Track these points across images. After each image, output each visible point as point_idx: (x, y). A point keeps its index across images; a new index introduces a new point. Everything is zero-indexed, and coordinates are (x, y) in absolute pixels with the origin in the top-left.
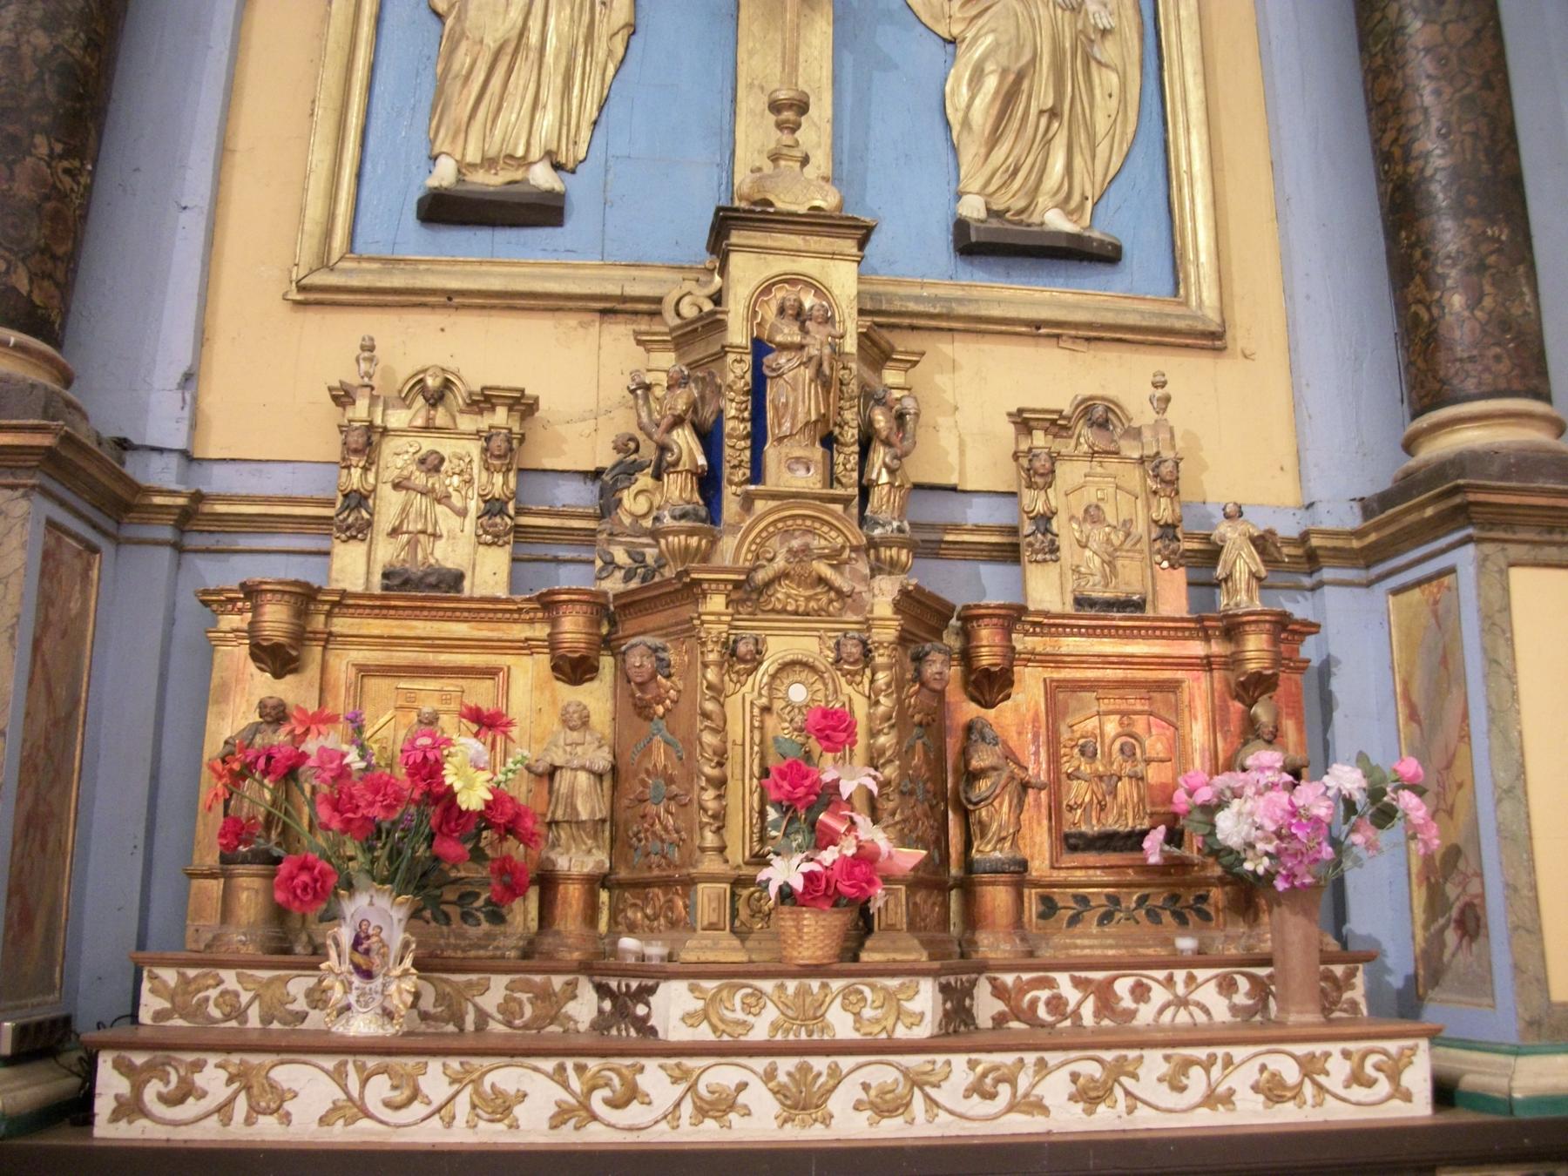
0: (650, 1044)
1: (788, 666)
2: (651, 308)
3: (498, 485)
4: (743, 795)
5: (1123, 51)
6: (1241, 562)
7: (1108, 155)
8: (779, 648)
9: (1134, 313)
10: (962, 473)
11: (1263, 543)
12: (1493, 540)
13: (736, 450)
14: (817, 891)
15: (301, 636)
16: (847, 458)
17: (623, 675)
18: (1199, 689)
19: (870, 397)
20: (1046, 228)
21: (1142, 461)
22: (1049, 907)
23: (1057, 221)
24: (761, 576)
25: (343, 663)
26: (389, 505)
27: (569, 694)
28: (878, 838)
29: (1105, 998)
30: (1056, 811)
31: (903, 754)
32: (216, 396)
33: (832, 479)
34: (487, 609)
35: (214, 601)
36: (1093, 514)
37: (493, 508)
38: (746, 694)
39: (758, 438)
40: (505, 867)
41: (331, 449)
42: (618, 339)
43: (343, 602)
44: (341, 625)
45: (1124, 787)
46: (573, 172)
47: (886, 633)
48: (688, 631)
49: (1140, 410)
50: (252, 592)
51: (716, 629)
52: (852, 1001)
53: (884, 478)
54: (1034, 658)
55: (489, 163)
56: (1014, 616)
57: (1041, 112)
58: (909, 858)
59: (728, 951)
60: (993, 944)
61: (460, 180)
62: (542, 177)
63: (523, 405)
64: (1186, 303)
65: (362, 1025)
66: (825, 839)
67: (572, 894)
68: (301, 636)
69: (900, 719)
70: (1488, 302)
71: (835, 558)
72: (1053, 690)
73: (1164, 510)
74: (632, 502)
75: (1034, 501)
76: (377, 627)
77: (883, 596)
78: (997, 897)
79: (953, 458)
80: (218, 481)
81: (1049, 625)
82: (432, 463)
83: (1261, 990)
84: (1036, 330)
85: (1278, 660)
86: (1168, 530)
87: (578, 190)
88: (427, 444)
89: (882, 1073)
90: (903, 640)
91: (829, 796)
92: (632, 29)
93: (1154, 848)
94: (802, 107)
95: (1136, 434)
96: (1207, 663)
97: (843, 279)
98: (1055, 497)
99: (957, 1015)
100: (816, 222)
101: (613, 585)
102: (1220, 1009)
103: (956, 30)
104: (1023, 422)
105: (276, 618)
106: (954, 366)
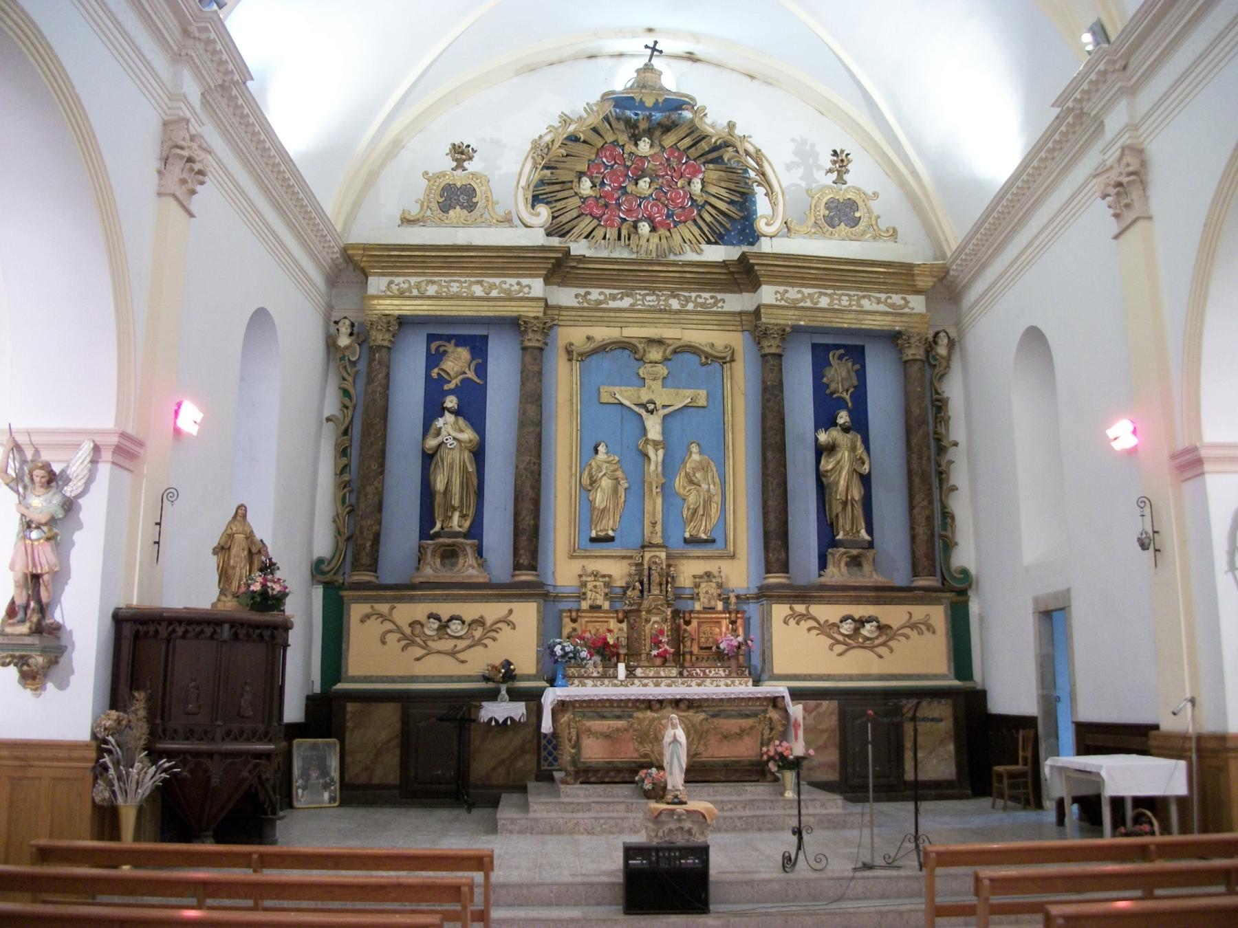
0: (635, 677)
1: (655, 622)
2: (631, 557)
3: (607, 590)
4: (648, 641)
5: (717, 499)
6: (733, 600)
7: (714, 520)
8: (654, 619)
9: (717, 553)
11: (738, 597)
13: (646, 586)
14: (659, 655)
15: (578, 616)
16: (664, 586)
17: (628, 622)
18: (725, 623)
19: (668, 575)
22: (697, 659)
23: (704, 536)
25: (584, 620)
26: (589, 594)
27: (620, 625)
28: (668, 648)
29: (704, 672)
30: (699, 643)
31: (672, 635)
32: (557, 575)
33: (661, 591)
34: (606, 612)
35: (562, 611)
36: (707, 592)
37: (606, 594)
38: (648, 627)
39: (649, 584)
40: (612, 652)
41: (578, 584)
42: (625, 563)
43: (584, 611)
44: (583, 614)
45: (711, 640)
47: (669, 617)
48: (639, 617)
49: (716, 574)
50: (570, 611)
51: (644, 617)
52: (664, 671)
54: (695, 618)
56: (691, 612)
58: (672, 650)
59: (647, 664)
60: (687, 664)
62: (611, 533)
63: (610, 576)
65: (595, 674)
66: (659, 648)
67: (622, 657)
68: (578, 616)
69: (672, 630)
71: (662, 605)
72: (699, 623)
73: (719, 591)
74: (629, 593)
75: (696, 591)
76: (589, 615)
77: (669, 611)
78: (688, 657)
80: (559, 590)
81: (699, 612)
82: (595, 587)
83: (730, 672)
85: (737, 618)
86: (720, 595)
88: (595, 583)
89: (668, 681)
90: (673, 617)
91: (661, 642)
93: (714, 649)
94: (656, 523)
95: (715, 577)
96: (725, 618)
97: (663, 555)
98: (700, 590)
99: (681, 674)
100: (657, 546)
101: (626, 608)
102: (723, 675)
104: (694, 577)
105: (574, 614)
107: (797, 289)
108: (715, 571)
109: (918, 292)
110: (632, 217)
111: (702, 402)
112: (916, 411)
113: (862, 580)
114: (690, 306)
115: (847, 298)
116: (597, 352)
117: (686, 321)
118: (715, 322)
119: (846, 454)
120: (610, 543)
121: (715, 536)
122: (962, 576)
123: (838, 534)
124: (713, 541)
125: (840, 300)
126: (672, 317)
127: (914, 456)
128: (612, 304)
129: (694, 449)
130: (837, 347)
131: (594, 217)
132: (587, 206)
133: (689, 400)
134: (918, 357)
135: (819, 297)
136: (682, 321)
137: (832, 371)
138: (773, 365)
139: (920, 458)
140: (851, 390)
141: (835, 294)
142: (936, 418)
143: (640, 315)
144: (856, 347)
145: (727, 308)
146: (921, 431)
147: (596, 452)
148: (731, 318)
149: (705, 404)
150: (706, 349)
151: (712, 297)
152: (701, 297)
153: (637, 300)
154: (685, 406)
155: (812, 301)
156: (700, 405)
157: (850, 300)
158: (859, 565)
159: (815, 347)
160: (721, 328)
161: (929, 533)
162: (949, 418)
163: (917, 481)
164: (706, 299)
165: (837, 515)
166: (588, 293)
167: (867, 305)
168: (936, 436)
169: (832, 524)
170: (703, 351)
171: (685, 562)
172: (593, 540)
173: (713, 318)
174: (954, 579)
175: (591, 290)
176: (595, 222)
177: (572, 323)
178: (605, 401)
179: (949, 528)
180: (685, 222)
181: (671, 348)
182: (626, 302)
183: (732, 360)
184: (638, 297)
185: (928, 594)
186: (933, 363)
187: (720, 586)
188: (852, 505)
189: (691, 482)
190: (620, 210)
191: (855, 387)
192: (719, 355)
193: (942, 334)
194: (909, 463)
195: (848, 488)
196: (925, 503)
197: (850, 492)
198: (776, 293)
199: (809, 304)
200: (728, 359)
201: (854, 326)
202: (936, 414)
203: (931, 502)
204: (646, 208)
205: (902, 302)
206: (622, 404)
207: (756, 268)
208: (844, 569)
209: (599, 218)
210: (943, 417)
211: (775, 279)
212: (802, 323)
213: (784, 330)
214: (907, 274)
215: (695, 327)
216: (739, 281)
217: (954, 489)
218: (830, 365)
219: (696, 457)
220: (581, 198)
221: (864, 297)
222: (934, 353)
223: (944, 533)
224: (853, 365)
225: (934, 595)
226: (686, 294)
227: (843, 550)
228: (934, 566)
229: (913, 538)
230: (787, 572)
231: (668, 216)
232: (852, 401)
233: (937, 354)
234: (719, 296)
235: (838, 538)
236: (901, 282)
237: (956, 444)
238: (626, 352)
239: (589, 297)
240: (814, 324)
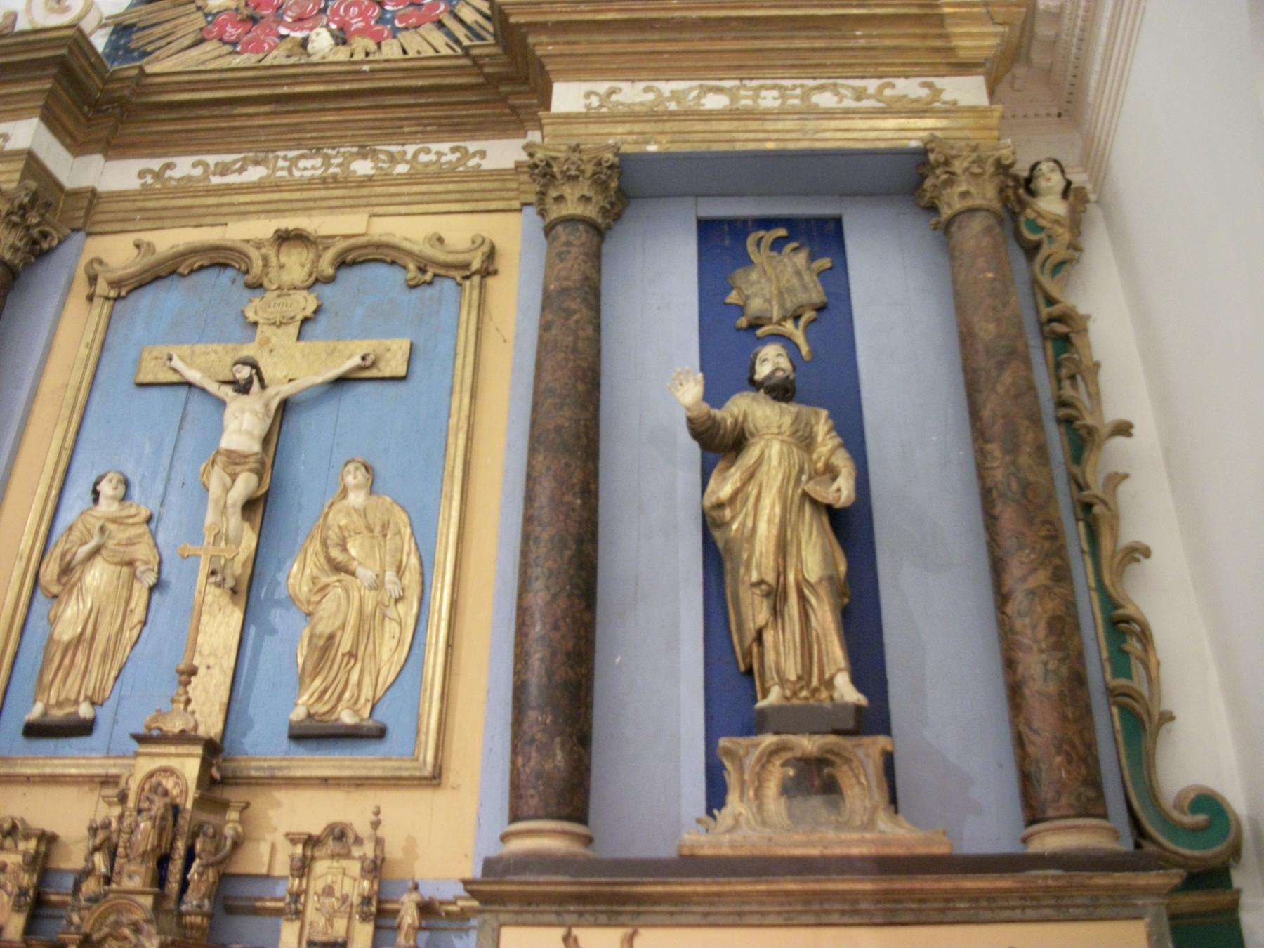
10: (270, 866)
12: (490, 911)
20: (339, 723)
21: (360, 858)
24: (96, 936)
36: (328, 891)
46: (102, 705)
53: (196, 877)
55: (59, 704)
57: (343, 655)
61: (45, 714)
62: (85, 711)
64: (417, 760)
70: (532, 763)
79: (266, 859)
84: (325, 782)
87: (104, 715)
92: (145, 623)
95: (358, 841)
103: (311, 608)
106: (279, 805)
107: (642, 85)
108: (360, 823)
109: (963, 67)
110: (302, 29)
111: (394, 365)
112: (986, 330)
113: (831, 834)
114: (402, 169)
115: (775, 93)
116: (158, 278)
117: (382, 200)
118: (457, 196)
119: (776, 448)
120: (76, 742)
121: (382, 716)
122: (1201, 818)
123: (765, 694)
124: (380, 734)
125: (756, 97)
126: (354, 192)
127: (994, 448)
128: (216, 180)
129: (354, 477)
130: (767, 223)
131: (225, 43)
132: (215, 25)
133: (356, 361)
134: (977, 202)
135: (699, 97)
136: (374, 200)
137: (754, 276)
138: (568, 244)
139: (1012, 449)
140: (809, 315)
141: (745, 86)
142: (1058, 366)
143: (276, 196)
144: (821, 222)
145: (487, 164)
146: (1007, 378)
147: (96, 495)
148: (498, 185)
149: (401, 371)
150: (416, 249)
151: (454, 150)
152: (428, 151)
153: (275, 169)
154: (342, 381)
155: (678, 103)
156: (387, 372)
157: (783, 97)
158: (831, 788)
159: (707, 228)
160: (467, 206)
161: (1064, 670)
162: (1097, 365)
163: (1008, 517)
164: (439, 154)
165: (759, 638)
166: (169, 166)
167: (825, 100)
168: (1063, 412)
169: (749, 672)
170: (409, 253)
171: (282, 795)
172: (35, 731)
173: (451, 187)
174: (1174, 829)
175: (177, 160)
176: (228, 48)
177: (118, 227)
178: (149, 378)
179: (1137, 668)
180: (416, 27)
181: (329, 255)
182: (254, 174)
183: (488, 272)
184: (281, 163)
185: (1081, 877)
186: (1032, 237)
187: (375, 868)
188: (802, 598)
189: (337, 568)
190: (280, 21)
191: (821, 309)
192: (450, 258)
193: (1044, 167)
194: (982, 470)
195: (782, 547)
196: (1042, 577)
197: (792, 561)
198: (588, 95)
199: (673, 106)
200: (476, 265)
201: (792, 146)
202: (1057, 354)
203: (1062, 575)
204: (336, 12)
205: (924, 93)
206: (189, 385)
207: (531, 40)
208: (774, 803)
209: (234, 44)
210: (1078, 363)
211: (581, 69)
212: (652, 148)
213: (599, 164)
214: (918, 19)
215: (403, 209)
216: (513, 101)
217: (1138, 552)
218: (747, 262)
219: (357, 498)
220: (206, 15)
221: (821, 88)
222: (1030, 214)
223: (1122, 682)
224: (812, 258)
225: (1102, 880)
226: (394, 149)
227: (768, 740)
228: (1094, 782)
229: (1015, 692)
230: (581, 816)
231: (381, 20)
232: (808, 340)
233: (1039, 214)
234: (472, 146)
235: (761, 704)
236: (916, 43)
237: (1124, 429)
238: (230, 273)
239: (168, 173)
240: (685, 148)
